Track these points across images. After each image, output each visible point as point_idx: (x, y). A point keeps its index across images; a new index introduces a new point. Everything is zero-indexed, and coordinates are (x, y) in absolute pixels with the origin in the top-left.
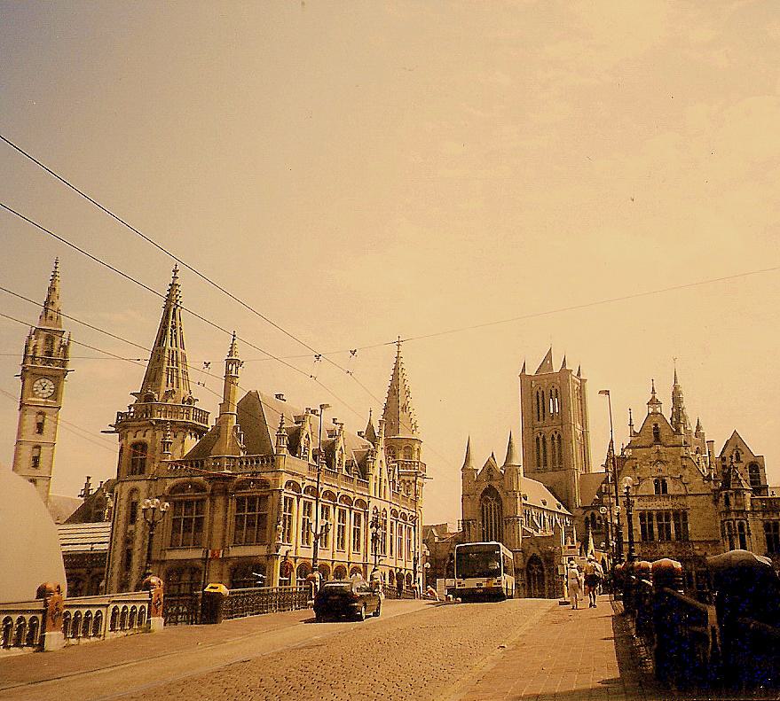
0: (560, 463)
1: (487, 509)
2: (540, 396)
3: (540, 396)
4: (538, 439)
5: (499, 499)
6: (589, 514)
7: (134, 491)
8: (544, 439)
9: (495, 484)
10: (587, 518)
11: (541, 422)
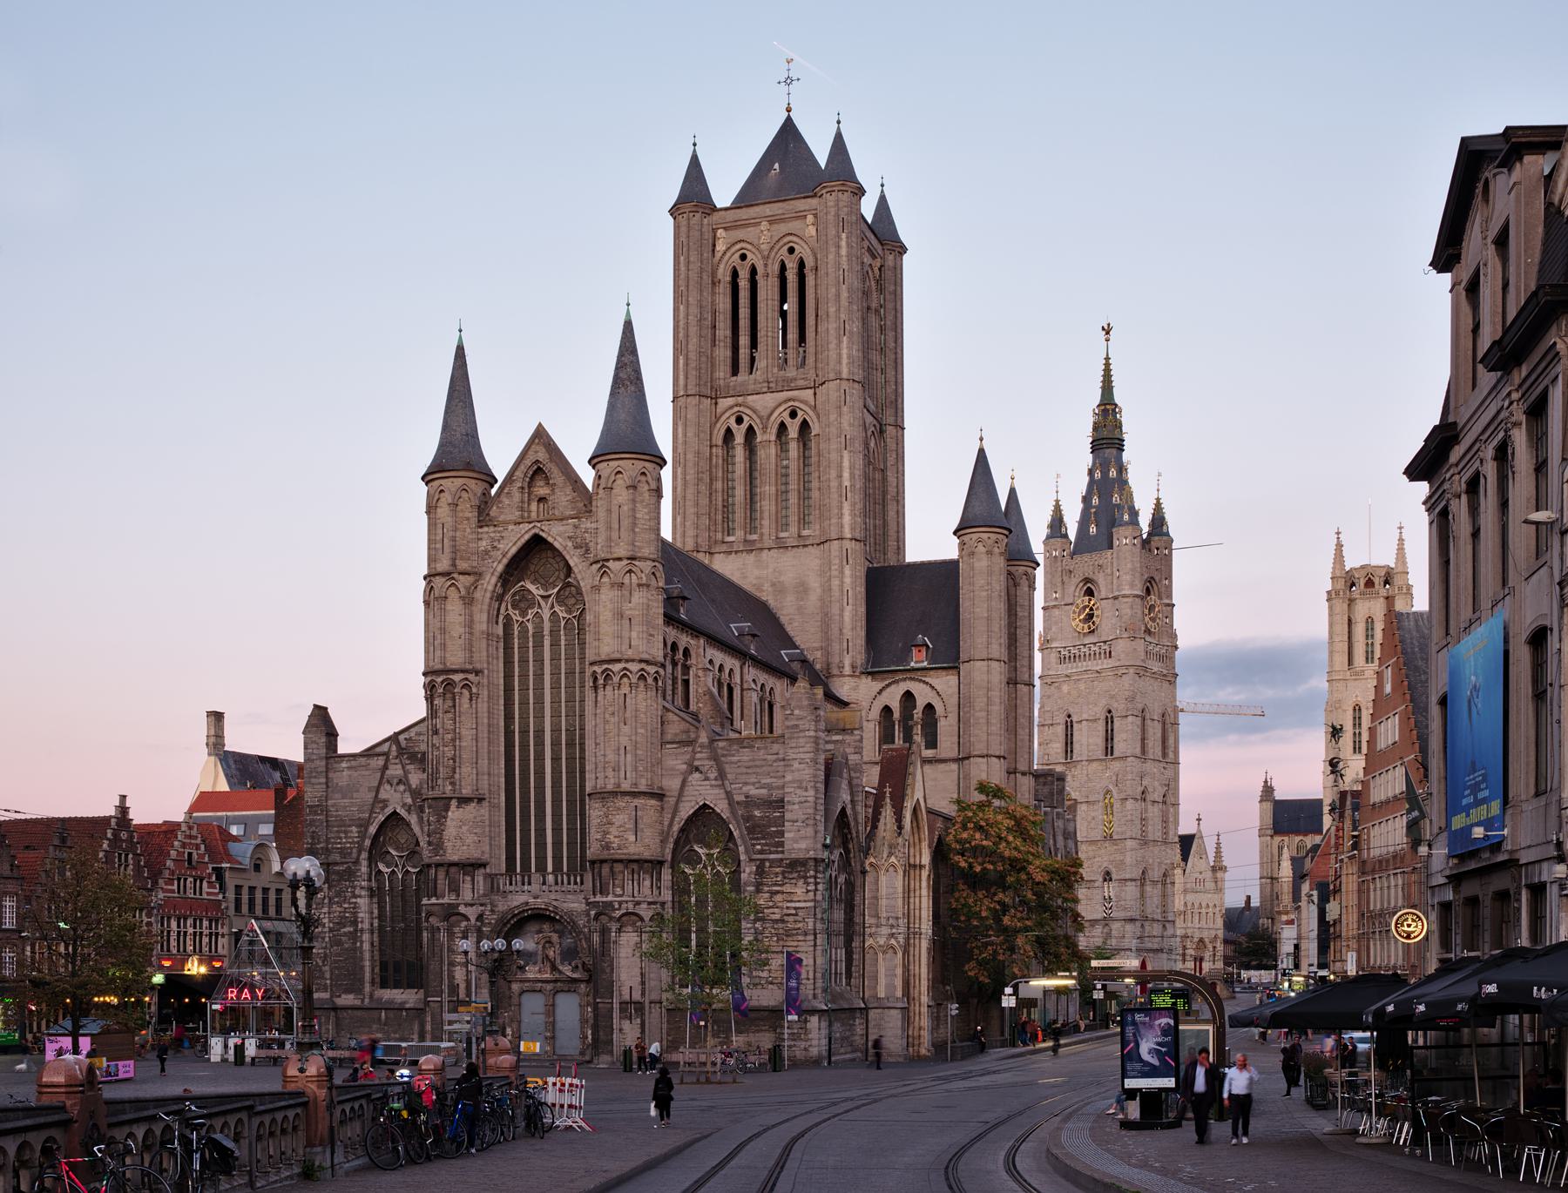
0: (804, 521)
1: (524, 631)
2: (743, 283)
3: (743, 283)
4: (729, 433)
5: (570, 593)
6: (893, 697)
8: (750, 431)
9: (556, 535)
10: (887, 710)
11: (743, 376)
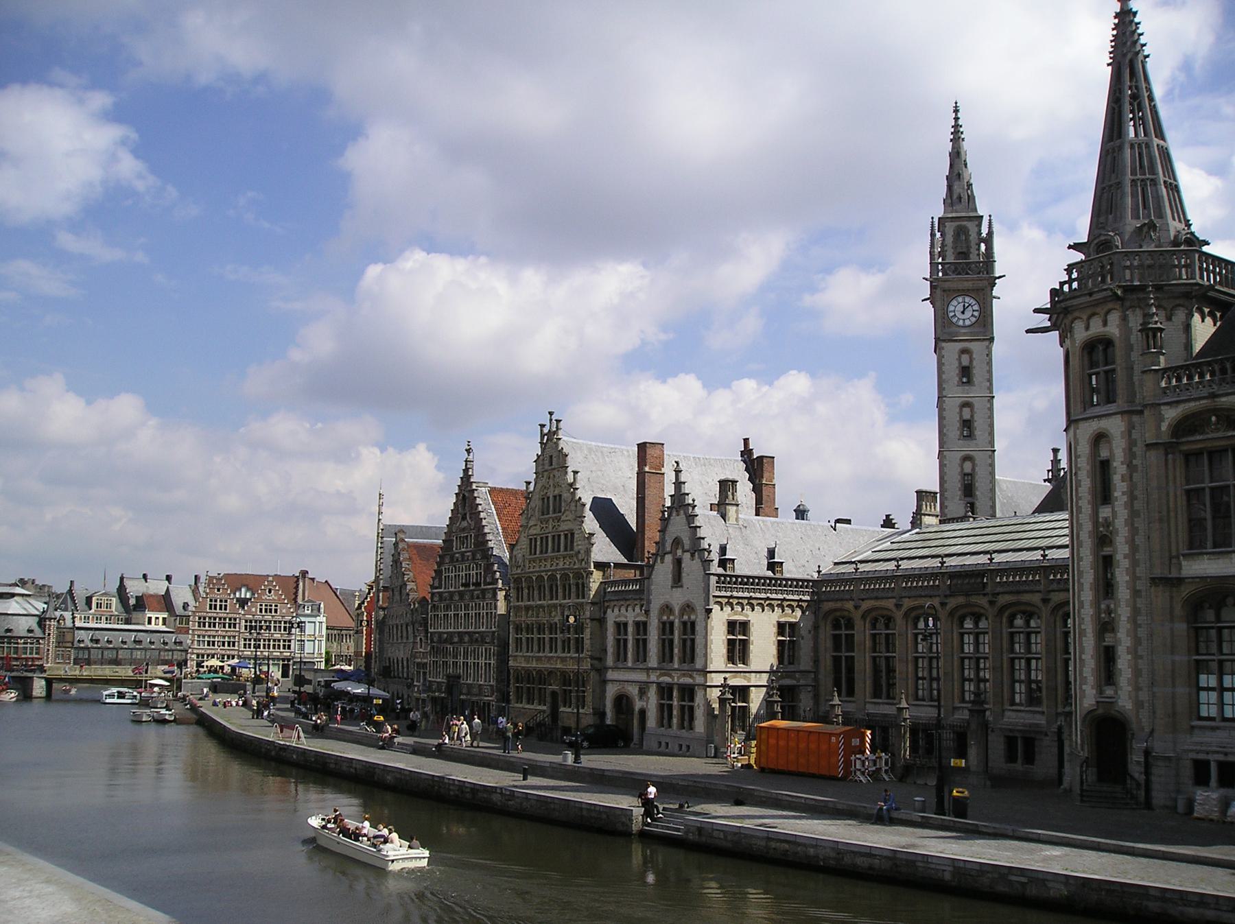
7: (1099, 438)
